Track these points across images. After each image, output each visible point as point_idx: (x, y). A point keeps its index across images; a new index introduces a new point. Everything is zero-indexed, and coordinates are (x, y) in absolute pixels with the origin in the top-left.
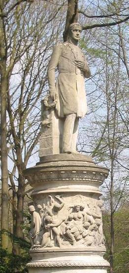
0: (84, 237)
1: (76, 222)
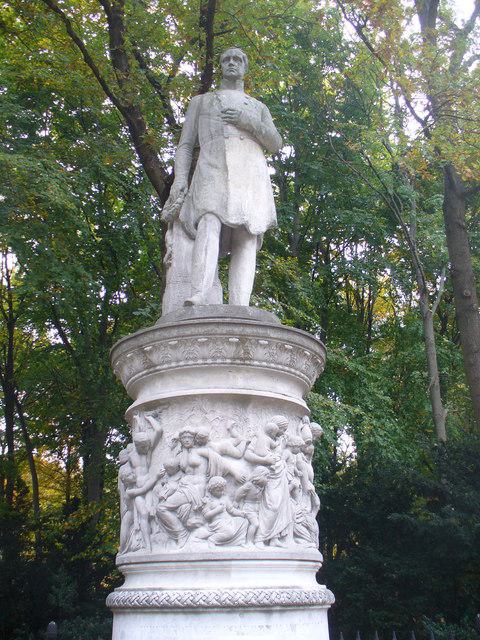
0: (210, 519)
1: (185, 479)
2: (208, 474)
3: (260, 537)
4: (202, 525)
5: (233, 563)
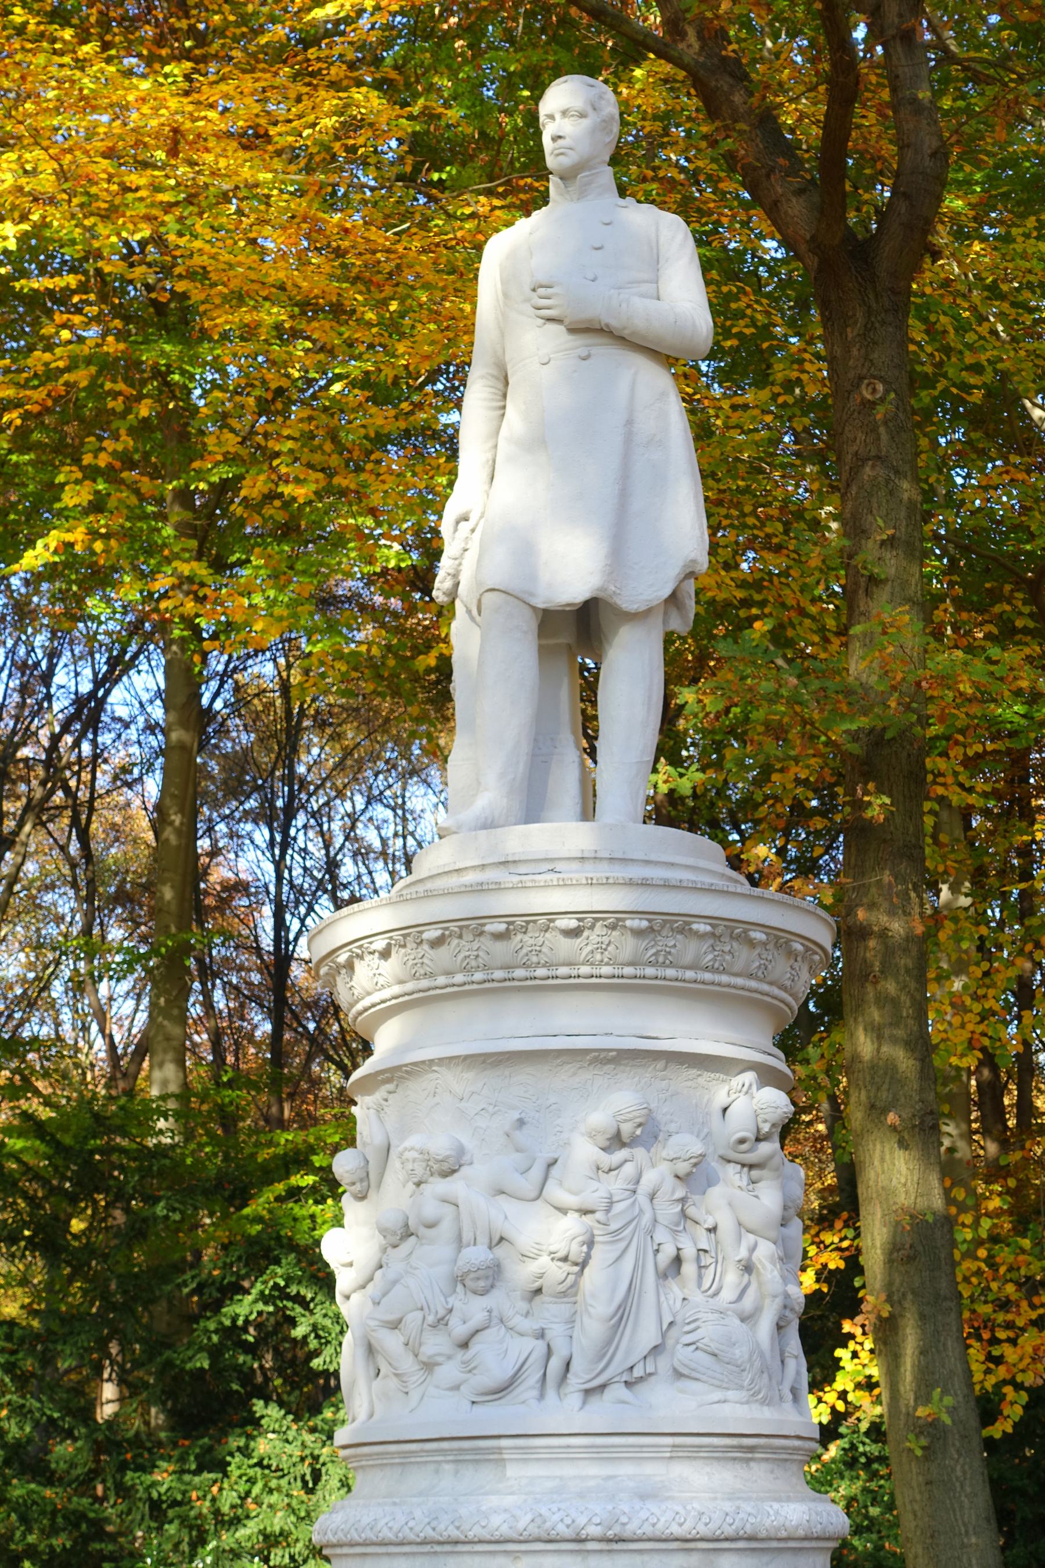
2: (460, 1243)
3: (576, 1380)
4: (449, 1357)
5: (504, 1443)
